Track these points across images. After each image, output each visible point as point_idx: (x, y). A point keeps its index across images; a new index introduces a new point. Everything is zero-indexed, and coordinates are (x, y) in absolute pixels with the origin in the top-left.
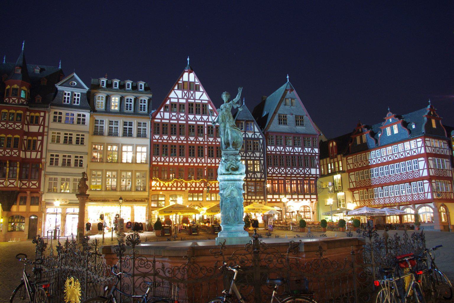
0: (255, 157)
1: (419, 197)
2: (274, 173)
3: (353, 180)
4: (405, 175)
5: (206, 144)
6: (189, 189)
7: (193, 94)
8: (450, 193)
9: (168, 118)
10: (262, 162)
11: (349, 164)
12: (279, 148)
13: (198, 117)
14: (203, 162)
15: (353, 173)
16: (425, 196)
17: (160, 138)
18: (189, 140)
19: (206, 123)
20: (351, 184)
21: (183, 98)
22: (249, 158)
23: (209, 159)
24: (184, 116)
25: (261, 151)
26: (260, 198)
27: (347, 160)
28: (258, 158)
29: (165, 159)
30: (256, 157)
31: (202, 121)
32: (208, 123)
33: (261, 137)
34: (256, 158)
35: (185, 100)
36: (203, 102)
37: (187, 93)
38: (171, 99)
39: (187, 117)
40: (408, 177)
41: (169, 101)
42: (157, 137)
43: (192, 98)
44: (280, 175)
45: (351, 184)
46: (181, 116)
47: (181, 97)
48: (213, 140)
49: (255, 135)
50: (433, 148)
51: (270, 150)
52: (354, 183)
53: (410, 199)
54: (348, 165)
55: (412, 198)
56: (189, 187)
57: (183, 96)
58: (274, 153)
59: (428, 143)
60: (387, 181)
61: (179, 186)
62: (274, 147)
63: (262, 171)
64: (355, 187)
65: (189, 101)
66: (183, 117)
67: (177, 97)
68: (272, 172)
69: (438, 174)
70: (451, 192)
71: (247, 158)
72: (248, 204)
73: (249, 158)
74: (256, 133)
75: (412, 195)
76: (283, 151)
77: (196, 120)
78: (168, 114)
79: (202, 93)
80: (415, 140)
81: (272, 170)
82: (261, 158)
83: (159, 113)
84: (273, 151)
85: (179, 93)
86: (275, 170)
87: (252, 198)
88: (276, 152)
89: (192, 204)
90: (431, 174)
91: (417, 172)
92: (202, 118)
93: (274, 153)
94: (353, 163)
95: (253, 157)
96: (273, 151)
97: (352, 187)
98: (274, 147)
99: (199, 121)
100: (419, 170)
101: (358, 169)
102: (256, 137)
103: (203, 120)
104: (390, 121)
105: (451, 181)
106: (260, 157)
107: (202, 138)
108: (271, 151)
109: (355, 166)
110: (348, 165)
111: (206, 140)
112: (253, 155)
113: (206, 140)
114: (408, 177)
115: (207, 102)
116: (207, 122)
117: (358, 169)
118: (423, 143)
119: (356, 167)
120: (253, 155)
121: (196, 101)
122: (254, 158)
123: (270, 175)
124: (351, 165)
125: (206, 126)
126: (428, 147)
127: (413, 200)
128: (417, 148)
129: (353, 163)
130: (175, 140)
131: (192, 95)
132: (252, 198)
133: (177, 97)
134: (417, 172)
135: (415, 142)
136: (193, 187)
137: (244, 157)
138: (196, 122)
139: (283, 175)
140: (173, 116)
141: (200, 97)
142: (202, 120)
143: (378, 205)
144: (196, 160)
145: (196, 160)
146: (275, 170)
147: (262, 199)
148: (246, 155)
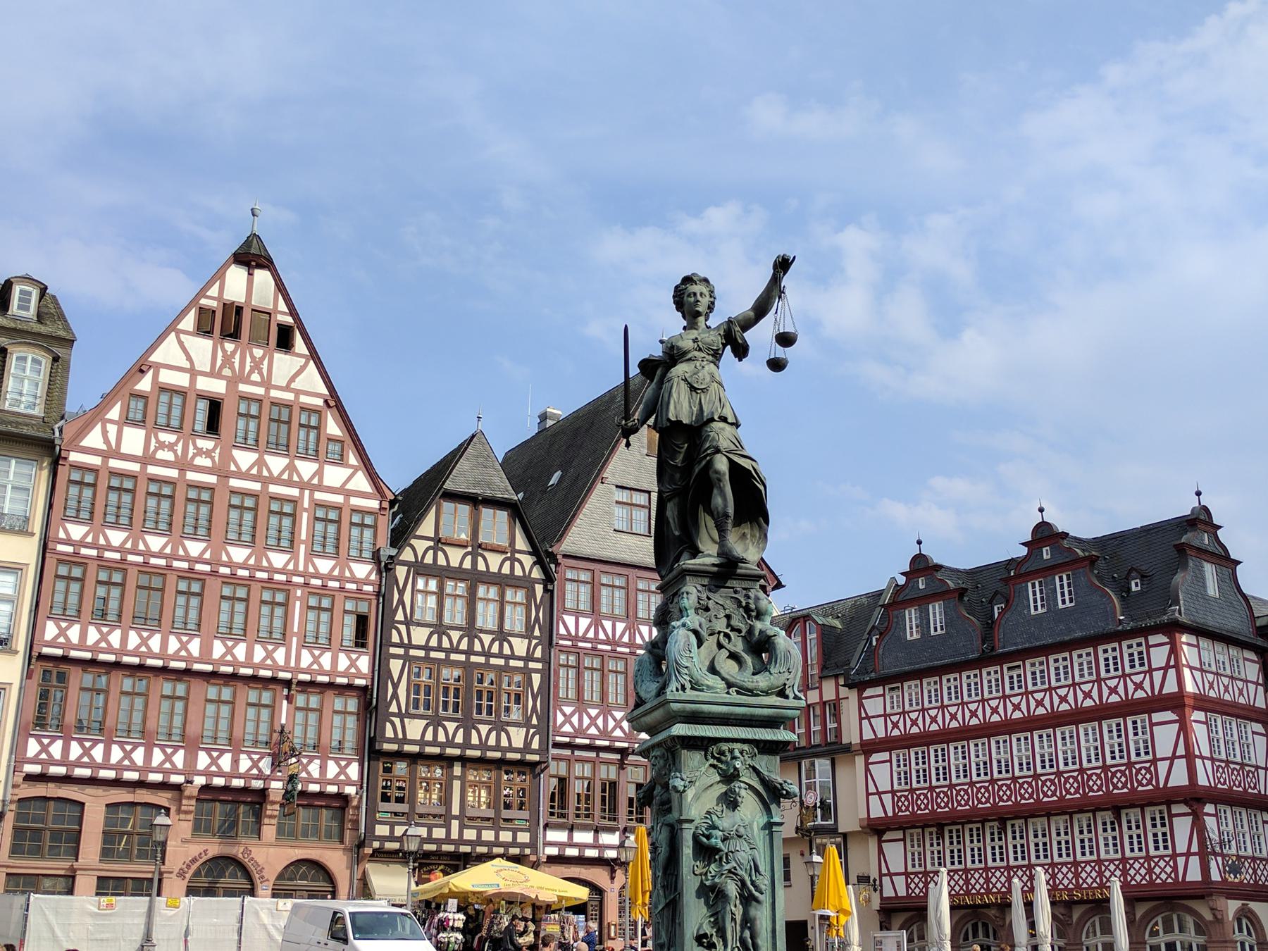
0: (507, 658)
1: (1150, 871)
2: (580, 732)
3: (884, 785)
4: (1098, 776)
5: (297, 585)
6: (200, 781)
7: (262, 358)
9: (139, 452)
10: (536, 679)
11: (868, 718)
12: (608, 624)
13: (276, 464)
14: (281, 662)
15: (885, 756)
16: (1175, 869)
17: (89, 539)
18: (224, 558)
19: (307, 492)
20: (874, 800)
21: (214, 374)
22: (482, 660)
23: (305, 653)
24: (214, 450)
25: (537, 633)
26: (515, 837)
27: (860, 699)
28: (520, 664)
29: (104, 637)
30: (513, 657)
31: (289, 483)
32: (319, 496)
33: (537, 573)
34: (513, 663)
35: (223, 383)
36: (304, 399)
37: (234, 353)
38: (163, 372)
39: (227, 458)
40: (1107, 787)
41: (150, 375)
42: (77, 531)
43: (255, 377)
44: (607, 743)
45: (874, 800)
46: (200, 452)
47: (208, 370)
49: (517, 564)
50: (1210, 677)
51: (573, 634)
52: (887, 798)
54: (865, 722)
56: (200, 774)
57: (219, 363)
58: (589, 645)
60: (1023, 797)
61: (155, 763)
62: (589, 620)
63: (534, 721)
64: (890, 814)
65: (243, 388)
66: (208, 453)
67: (187, 365)
68: (572, 725)
69: (1225, 783)
71: (474, 659)
72: (461, 863)
73: (482, 660)
74: (517, 555)
76: (626, 639)
77: (265, 473)
78: (141, 433)
79: (303, 360)
80: (1142, 640)
82: (532, 665)
83: (98, 427)
84: (585, 639)
85: (202, 348)
86: (586, 721)
87: (479, 835)
88: (596, 640)
91: (1148, 770)
92: (291, 468)
93: (589, 645)
94: (885, 716)
95: (500, 655)
96: (585, 639)
97: (877, 813)
98: (589, 620)
99: (278, 481)
100: (1154, 761)
101: (906, 742)
103: (296, 478)
104: (1045, 557)
106: (529, 658)
107: (286, 557)
108: (576, 638)
109: (895, 725)
110: (865, 722)
111: (301, 568)
112: (501, 647)
113: (301, 568)
114: (1107, 787)
115: (320, 402)
116: (313, 489)
117: (906, 742)
119: (896, 733)
120: (501, 647)
121: (274, 393)
122: (501, 662)
123: (567, 740)
124: (879, 724)
125: (306, 505)
128: (1151, 671)
129: (885, 716)
130: (159, 555)
131: (257, 365)
132: (479, 835)
133: (187, 365)
134: (1148, 770)
135: (1143, 648)
136: (220, 774)
137: (462, 652)
138: (266, 482)
139: (618, 744)
140: (162, 445)
141: (293, 379)
142: (291, 476)
143: (982, 895)
144: (250, 653)
147: (522, 846)
148: (471, 644)
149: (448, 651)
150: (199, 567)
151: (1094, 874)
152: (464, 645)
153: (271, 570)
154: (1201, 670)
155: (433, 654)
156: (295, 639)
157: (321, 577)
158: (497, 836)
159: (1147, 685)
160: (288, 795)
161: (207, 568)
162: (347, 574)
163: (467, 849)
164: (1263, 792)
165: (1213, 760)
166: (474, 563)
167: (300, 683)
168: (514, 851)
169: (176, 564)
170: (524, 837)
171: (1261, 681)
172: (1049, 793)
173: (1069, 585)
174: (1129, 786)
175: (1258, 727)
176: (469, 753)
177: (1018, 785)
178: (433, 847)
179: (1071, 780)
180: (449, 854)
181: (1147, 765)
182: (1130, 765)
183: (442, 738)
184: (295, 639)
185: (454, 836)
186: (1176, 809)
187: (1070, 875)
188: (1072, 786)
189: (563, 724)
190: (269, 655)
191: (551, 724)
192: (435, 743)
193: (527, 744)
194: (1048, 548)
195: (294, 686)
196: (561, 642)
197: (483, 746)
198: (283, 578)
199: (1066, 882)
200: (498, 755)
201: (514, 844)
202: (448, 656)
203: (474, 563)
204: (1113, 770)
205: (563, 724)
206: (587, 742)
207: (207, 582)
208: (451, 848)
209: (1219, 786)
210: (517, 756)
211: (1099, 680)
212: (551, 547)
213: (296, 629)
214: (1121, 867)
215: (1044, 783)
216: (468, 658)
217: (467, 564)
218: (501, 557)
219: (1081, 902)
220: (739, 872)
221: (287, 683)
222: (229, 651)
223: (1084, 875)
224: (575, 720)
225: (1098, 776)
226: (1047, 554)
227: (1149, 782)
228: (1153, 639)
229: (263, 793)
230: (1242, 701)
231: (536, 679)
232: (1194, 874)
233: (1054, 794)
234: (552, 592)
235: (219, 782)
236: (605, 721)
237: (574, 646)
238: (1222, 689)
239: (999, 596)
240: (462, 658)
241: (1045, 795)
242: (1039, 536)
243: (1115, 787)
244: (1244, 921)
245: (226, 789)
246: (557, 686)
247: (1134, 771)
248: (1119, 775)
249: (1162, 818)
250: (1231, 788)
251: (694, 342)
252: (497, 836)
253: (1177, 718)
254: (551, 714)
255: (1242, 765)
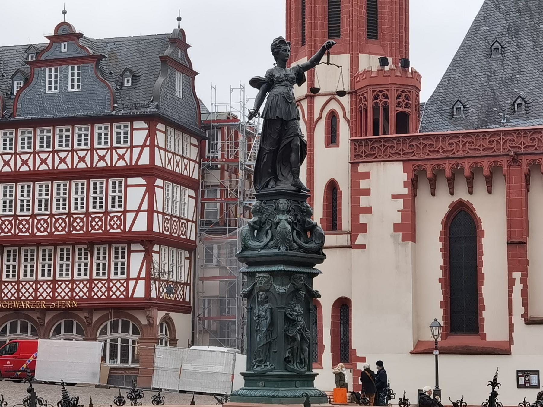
1: (109, 289)
4: (82, 219)
8: (184, 284)
16: (127, 289)
50: (170, 155)
53: (81, 294)
55: (90, 289)
59: (160, 138)
60: (20, 231)
70: (186, 284)
75: (91, 281)
90: (156, 229)
100: (125, 212)
104: (63, 50)
105: (190, 255)
118: (148, 135)
126: (160, 148)
127: (90, 298)
128: (132, 147)
134: (119, 218)
135: (129, 130)
151: (67, 290)
154: (165, 150)
159: (127, 157)
164: (188, 238)
165: (163, 214)
171: (198, 160)
172: (42, 229)
173: (79, 75)
174: (103, 228)
175: (192, 193)
177: (18, 222)
179: (60, 221)
181: (119, 214)
182: (106, 213)
186: (133, 247)
187: (49, 290)
188: (60, 225)
194: (66, 43)
199: (45, 295)
204: (93, 216)
209: (165, 232)
211: (92, 149)
214: (88, 286)
215: (39, 221)
219: (55, 309)
223: (59, 290)
225: (82, 219)
226: (65, 48)
227: (119, 227)
228: (136, 125)
230: (186, 173)
232: (140, 293)
233: (46, 230)
238: (175, 164)
239: (19, 74)
241: (39, 230)
242: (59, 33)
243: (93, 228)
244: (165, 325)
247: (109, 218)
248: (97, 220)
249: (123, 253)
250: (171, 234)
251: (285, 76)
253: (146, 183)
255: (180, 218)
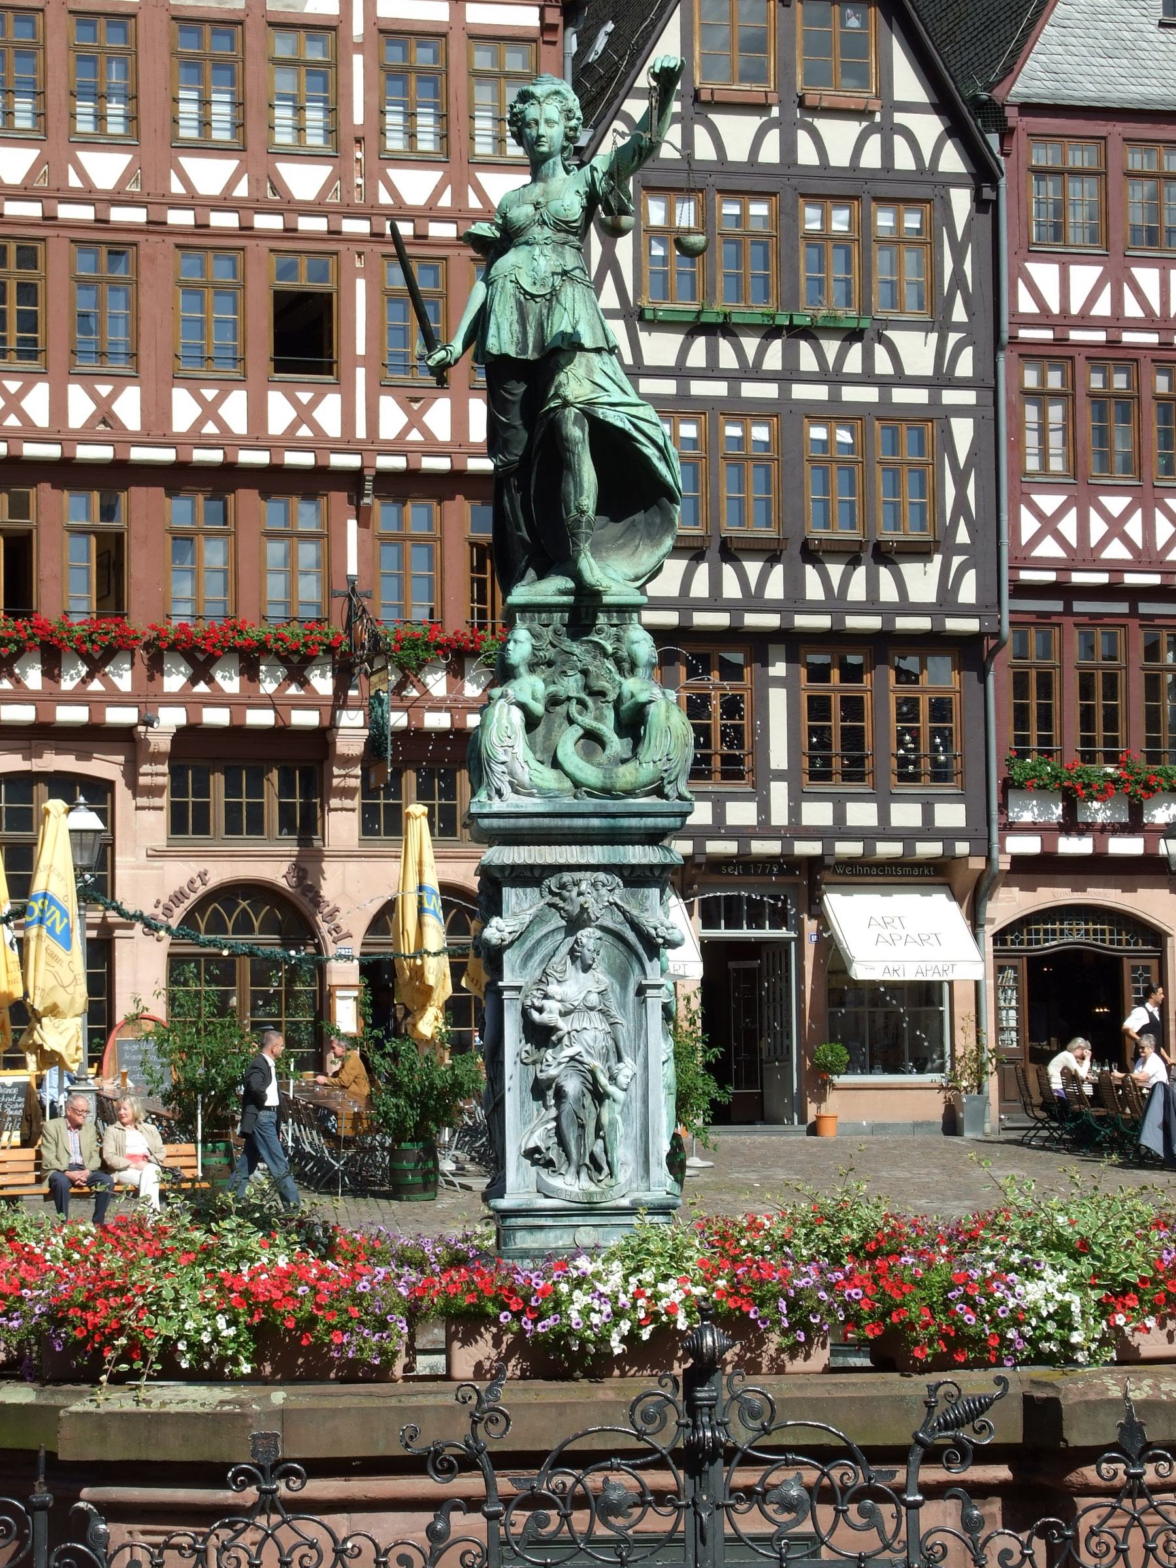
0: (884, 384)
2: (1083, 556)
6: (172, 718)
10: (963, 431)
18: (177, 187)
22: (820, 392)
25: (959, 314)
26: (928, 815)
28: (920, 396)
30: (902, 380)
33: (952, 161)
34: (900, 395)
44: (1155, 579)
48: (437, 193)
49: (899, 142)
51: (1055, 309)
62: (1098, 270)
63: (963, 536)
71: (800, 392)
73: (820, 392)
74: (899, 118)
81: (1068, 526)
82: (950, 397)
84: (1085, 321)
88: (1117, 322)
89: (202, 876)
93: (1100, 336)
95: (867, 378)
98: (1098, 270)
102: (904, 160)
106: (942, 379)
108: (1064, 321)
123: (1051, 576)
132: (840, 815)
144: (257, 413)
145: (257, 413)
146: (1098, 528)
147: (949, 836)
148: (791, 357)
149: (733, 378)
150: (119, 215)
152: (774, 359)
153: (290, 207)
155: (699, 388)
156: (361, 373)
157: (411, 215)
158: (884, 815)
160: (375, 746)
161: (138, 215)
162: (474, 202)
163: (812, 848)
166: (788, 147)
167: (383, 476)
168: (929, 849)
169: (66, 212)
170: (951, 815)
176: (803, 621)
178: (729, 847)
180: (769, 860)
183: (731, 589)
184: (361, 373)
185: (779, 816)
189: (1036, 539)
190: (304, 415)
191: (1005, 539)
192: (715, 602)
193: (947, 591)
195: (368, 486)
196: (1024, 334)
197: (836, 603)
198: (318, 224)
200: (873, 623)
201: (928, 831)
202: (734, 391)
203: (788, 147)
205: (1036, 539)
206: (1103, 578)
207: (144, 249)
208: (773, 847)
210: (923, 623)
212: (990, 87)
213: (361, 349)
216: (785, 392)
217: (770, 153)
218: (853, 128)
220: (586, 1059)
221: (351, 480)
222: (210, 411)
224: (1068, 526)
229: (323, 736)
231: (963, 431)
234: (996, 203)
235: (216, 717)
236: (1149, 526)
237: (1061, 341)
240: (770, 391)
245: (237, 732)
246: (1018, 447)
252: (884, 815)
254: (1004, 517)
